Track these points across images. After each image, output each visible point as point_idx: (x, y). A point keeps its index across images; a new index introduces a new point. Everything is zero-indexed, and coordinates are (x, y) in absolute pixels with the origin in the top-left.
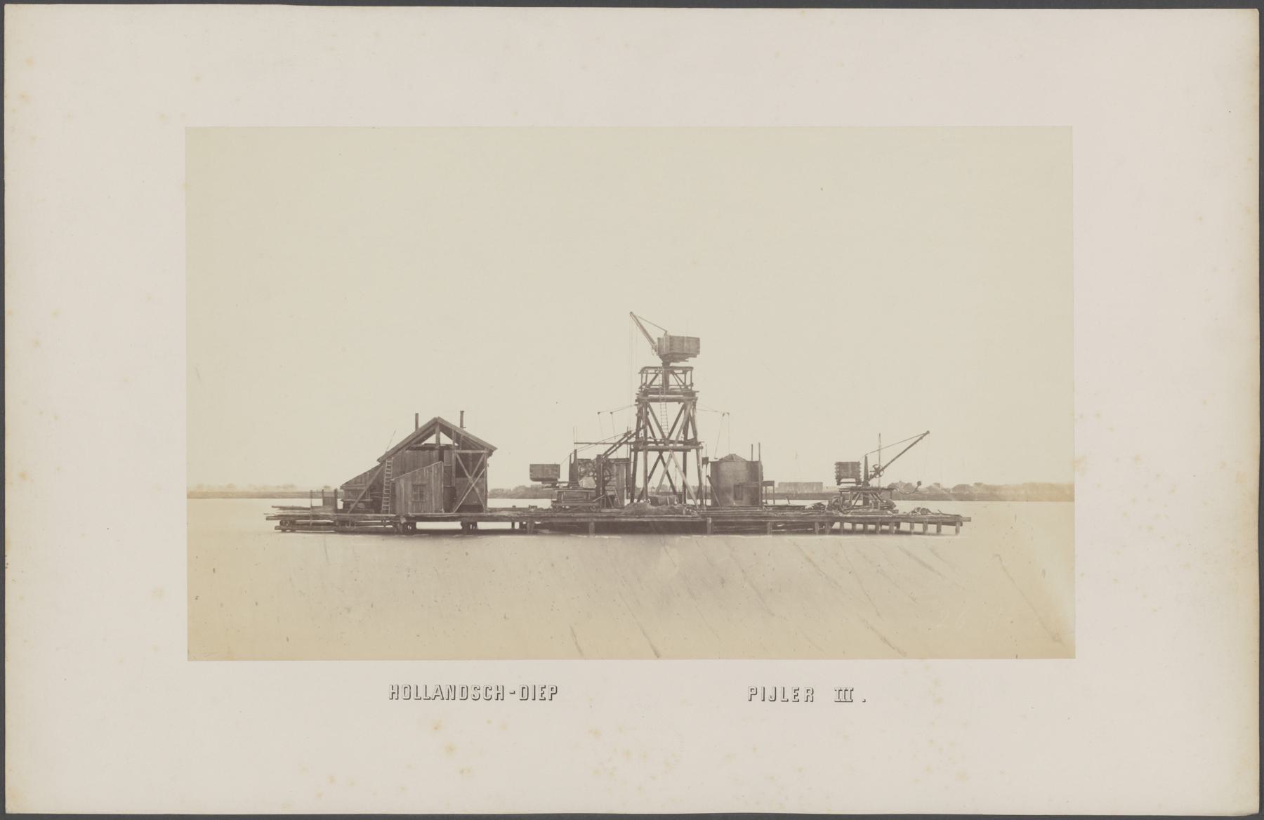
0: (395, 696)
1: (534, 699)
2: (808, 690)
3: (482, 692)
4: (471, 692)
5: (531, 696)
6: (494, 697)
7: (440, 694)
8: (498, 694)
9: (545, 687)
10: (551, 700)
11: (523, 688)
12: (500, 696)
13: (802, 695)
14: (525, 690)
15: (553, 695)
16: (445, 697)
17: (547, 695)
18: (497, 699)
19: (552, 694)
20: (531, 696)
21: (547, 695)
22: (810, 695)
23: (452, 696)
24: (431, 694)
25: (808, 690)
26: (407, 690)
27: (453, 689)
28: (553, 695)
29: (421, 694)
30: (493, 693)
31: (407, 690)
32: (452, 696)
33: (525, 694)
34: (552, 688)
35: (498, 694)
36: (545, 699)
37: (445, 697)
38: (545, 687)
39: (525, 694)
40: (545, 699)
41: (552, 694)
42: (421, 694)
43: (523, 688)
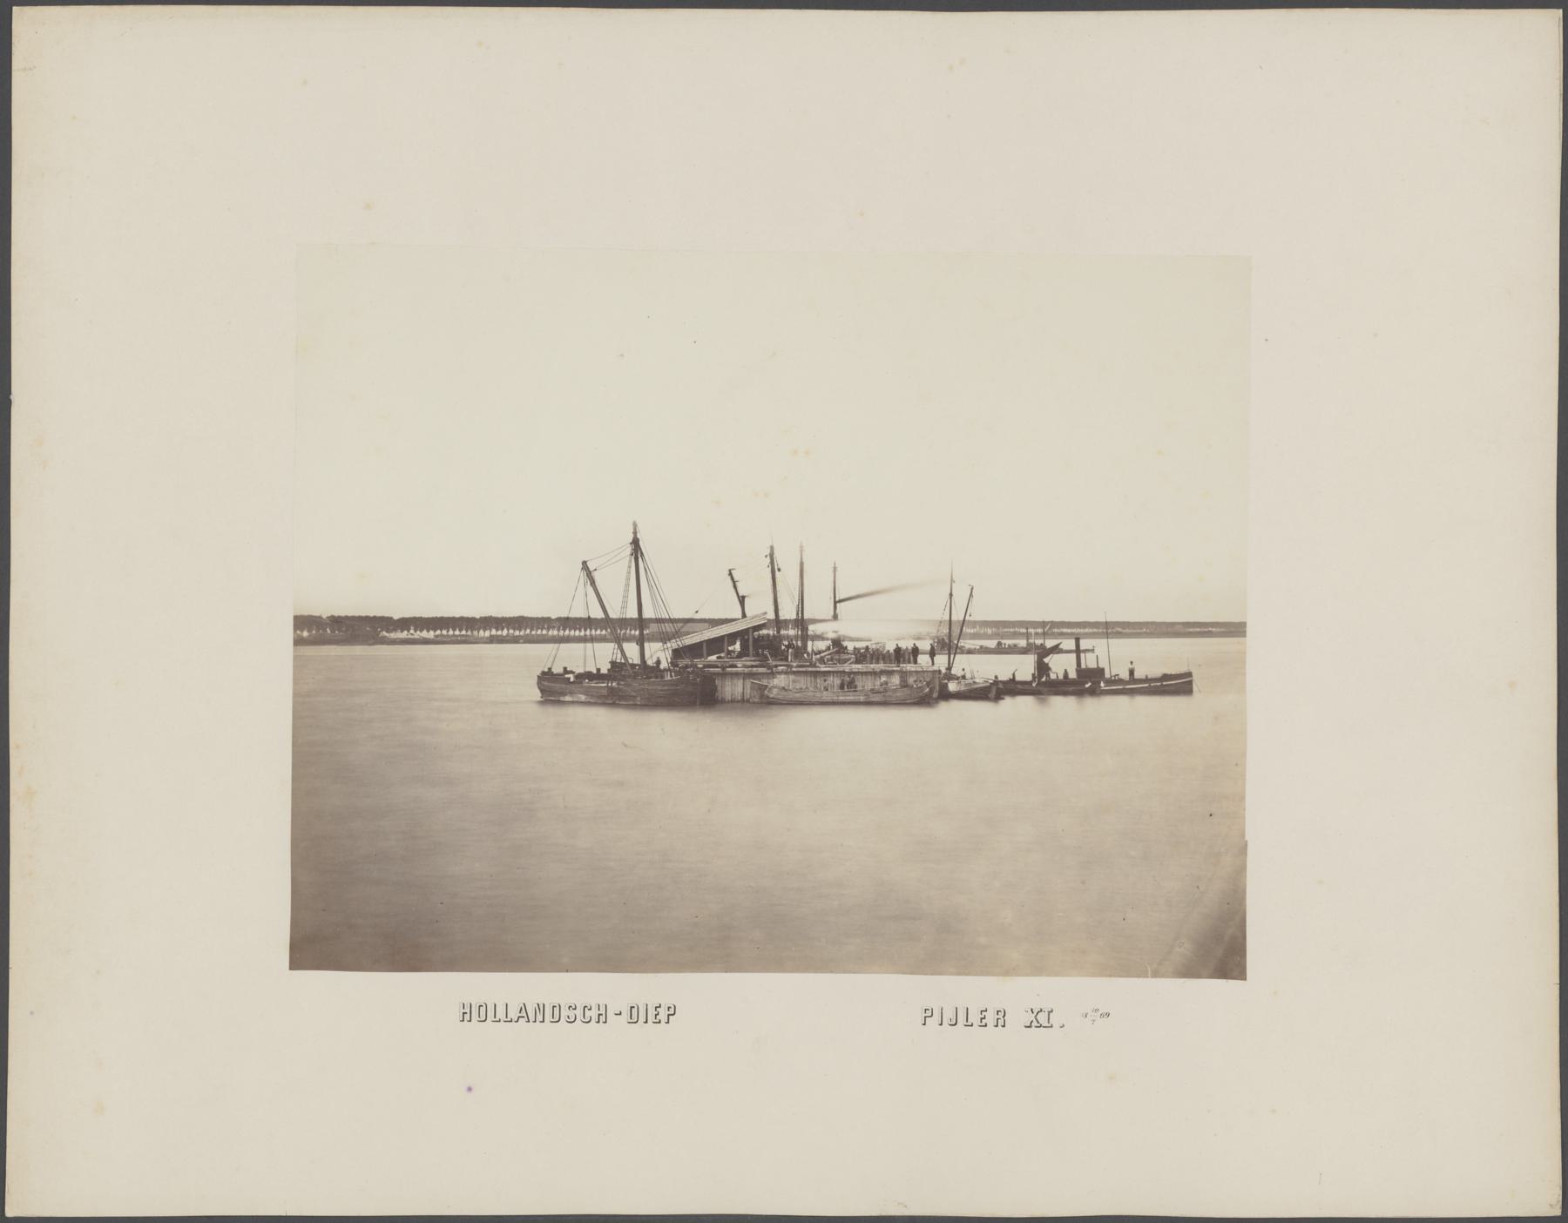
0: (467, 1017)
1: (646, 1022)
2: (998, 1012)
3: (579, 1012)
4: (565, 1013)
5: (642, 1018)
6: (595, 1018)
7: (524, 1014)
8: (599, 1015)
9: (660, 1007)
10: (668, 1022)
11: (632, 1007)
12: (602, 1018)
13: (991, 1018)
14: (635, 1011)
15: (671, 1017)
16: (532, 1018)
17: (663, 1016)
18: (598, 1022)
19: (669, 1015)
20: (642, 1018)
21: (663, 1016)
22: (1001, 1022)
23: (540, 1018)
24: (513, 1014)
25: (998, 1012)
26: (483, 1009)
27: (541, 1008)
28: (671, 1017)
29: (501, 1014)
30: (593, 1014)
31: (483, 1009)
32: (540, 1018)
33: (634, 1015)
34: (669, 1008)
35: (599, 1015)
36: (660, 1022)
37: (532, 1018)
38: (660, 1007)
39: (634, 1015)
40: (660, 1022)
41: (669, 1015)
42: (501, 1014)
43: (632, 1007)
